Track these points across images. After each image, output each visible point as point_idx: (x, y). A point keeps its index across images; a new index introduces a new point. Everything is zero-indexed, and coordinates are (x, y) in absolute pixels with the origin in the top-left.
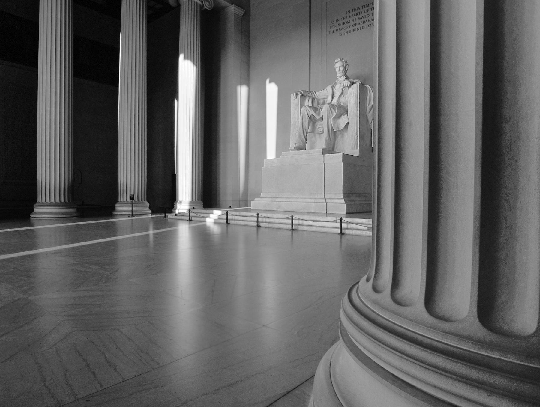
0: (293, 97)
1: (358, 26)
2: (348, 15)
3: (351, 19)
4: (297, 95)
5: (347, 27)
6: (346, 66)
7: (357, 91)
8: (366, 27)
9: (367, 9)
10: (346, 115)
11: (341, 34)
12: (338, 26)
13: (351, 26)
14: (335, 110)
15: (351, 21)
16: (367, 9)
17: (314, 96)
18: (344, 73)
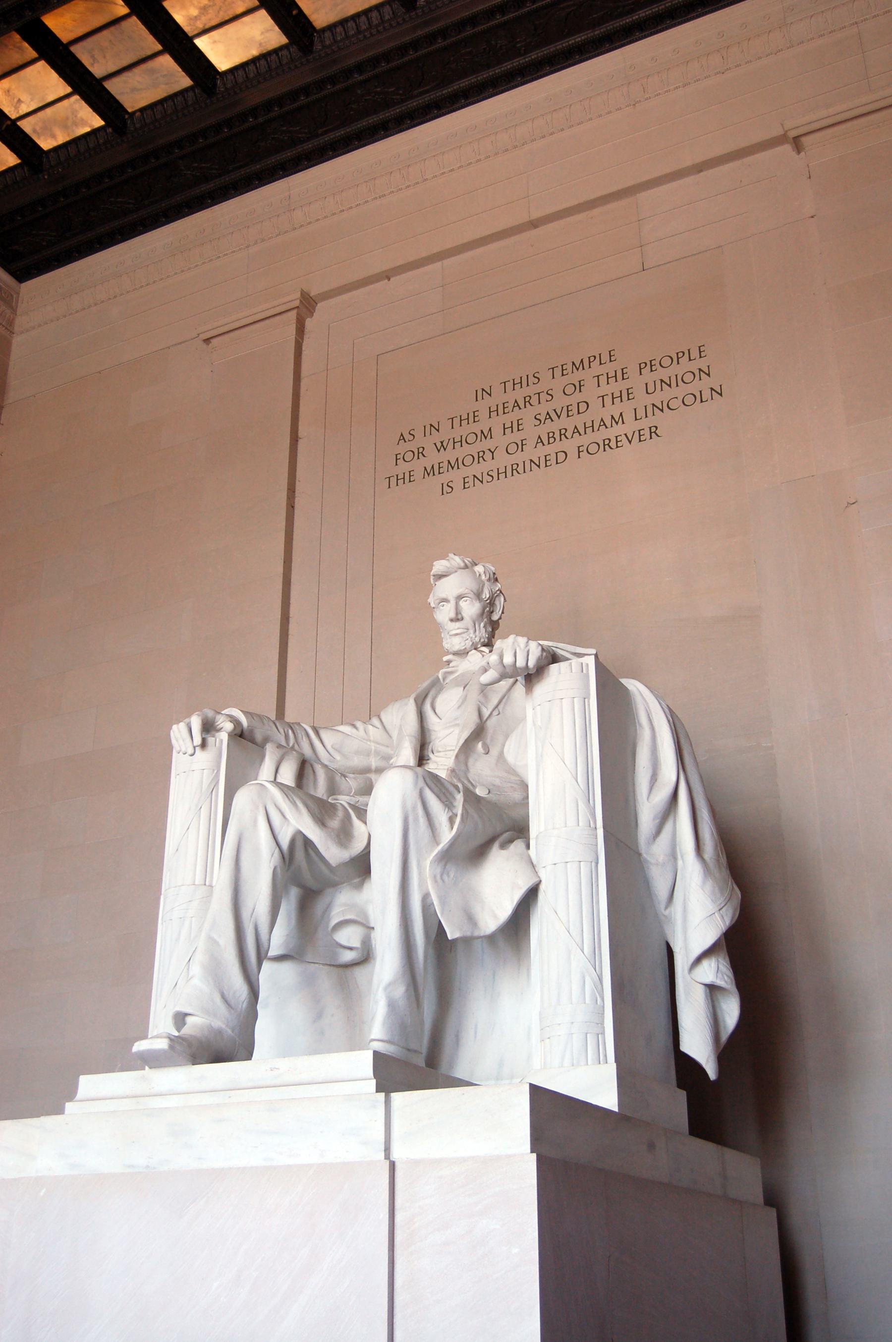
0: (182, 736)
1: (532, 452)
3: (497, 423)
4: (208, 727)
5: (481, 457)
6: (491, 603)
7: (585, 699)
8: (573, 453)
10: (517, 846)
11: (447, 488)
12: (430, 450)
13: (500, 454)
14: (448, 803)
15: (497, 431)
17: (307, 751)
18: (482, 633)
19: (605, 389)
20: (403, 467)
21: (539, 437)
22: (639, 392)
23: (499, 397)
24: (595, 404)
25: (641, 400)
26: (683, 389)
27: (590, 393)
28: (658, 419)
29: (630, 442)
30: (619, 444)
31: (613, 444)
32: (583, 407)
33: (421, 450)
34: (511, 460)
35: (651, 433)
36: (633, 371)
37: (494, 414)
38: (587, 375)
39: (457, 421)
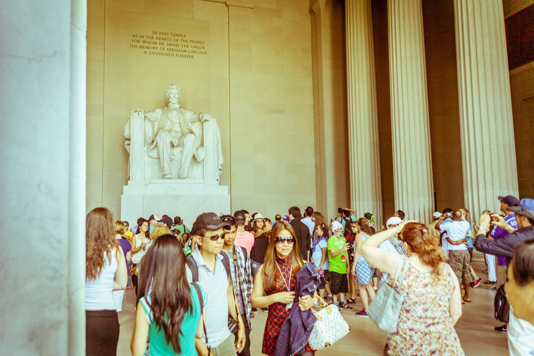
2: (155, 36)
3: (158, 41)
5: (154, 48)
8: (175, 55)
9: (177, 38)
11: (145, 53)
12: (141, 41)
13: (158, 49)
15: (158, 43)
20: (134, 43)
22: (190, 46)
23: (158, 35)
24: (181, 46)
25: (190, 49)
26: (199, 50)
27: (179, 42)
34: (161, 51)
36: (189, 41)
38: (179, 38)
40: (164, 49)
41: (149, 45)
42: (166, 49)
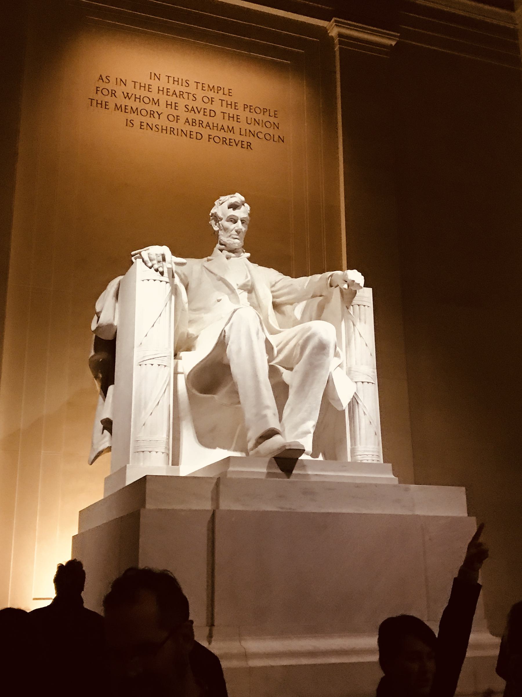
3: (163, 99)
5: (152, 114)
8: (206, 137)
9: (211, 94)
11: (130, 123)
13: (164, 117)
15: (162, 103)
16: (211, 94)
19: (224, 109)
20: (99, 97)
21: (187, 119)
22: (242, 119)
23: (163, 83)
24: (219, 115)
25: (244, 126)
26: (264, 130)
28: (251, 139)
29: (237, 145)
30: (231, 144)
31: (228, 142)
32: (213, 114)
33: (113, 92)
35: (248, 146)
36: (240, 106)
37: (161, 92)
38: (217, 97)
39: (138, 85)
40: (177, 118)
41: (140, 106)
42: (182, 120)
